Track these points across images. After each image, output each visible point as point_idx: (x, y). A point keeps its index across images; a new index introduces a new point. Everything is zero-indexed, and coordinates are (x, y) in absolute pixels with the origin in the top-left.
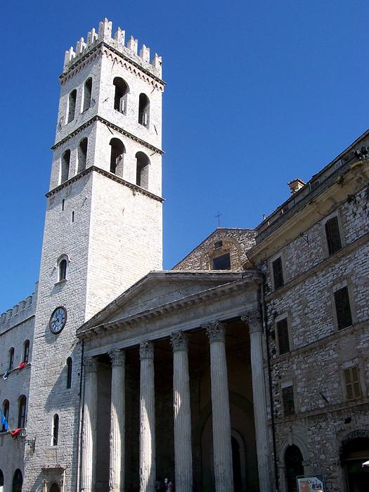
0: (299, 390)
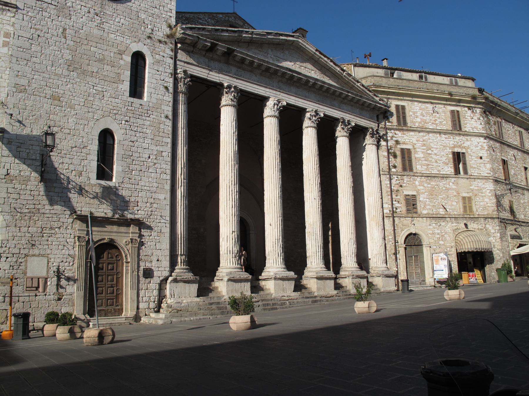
0: (421, 199)
